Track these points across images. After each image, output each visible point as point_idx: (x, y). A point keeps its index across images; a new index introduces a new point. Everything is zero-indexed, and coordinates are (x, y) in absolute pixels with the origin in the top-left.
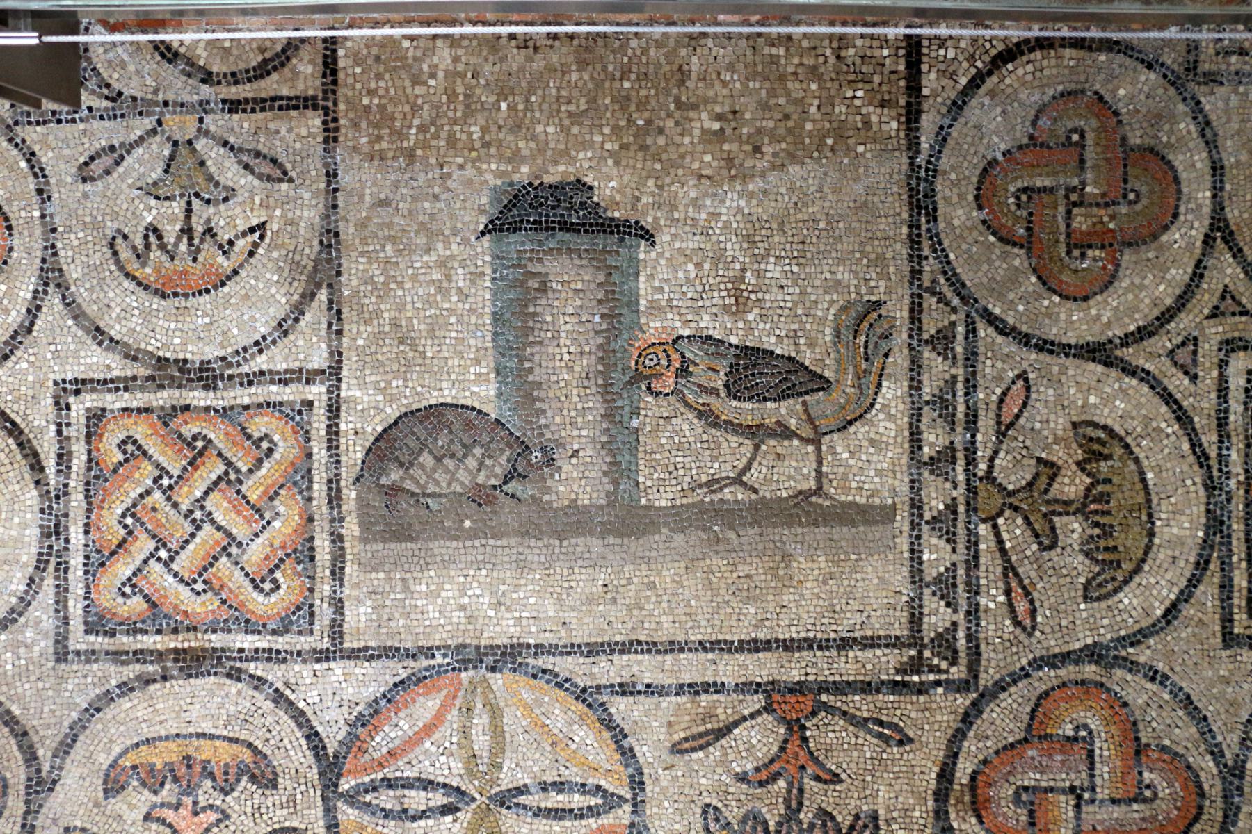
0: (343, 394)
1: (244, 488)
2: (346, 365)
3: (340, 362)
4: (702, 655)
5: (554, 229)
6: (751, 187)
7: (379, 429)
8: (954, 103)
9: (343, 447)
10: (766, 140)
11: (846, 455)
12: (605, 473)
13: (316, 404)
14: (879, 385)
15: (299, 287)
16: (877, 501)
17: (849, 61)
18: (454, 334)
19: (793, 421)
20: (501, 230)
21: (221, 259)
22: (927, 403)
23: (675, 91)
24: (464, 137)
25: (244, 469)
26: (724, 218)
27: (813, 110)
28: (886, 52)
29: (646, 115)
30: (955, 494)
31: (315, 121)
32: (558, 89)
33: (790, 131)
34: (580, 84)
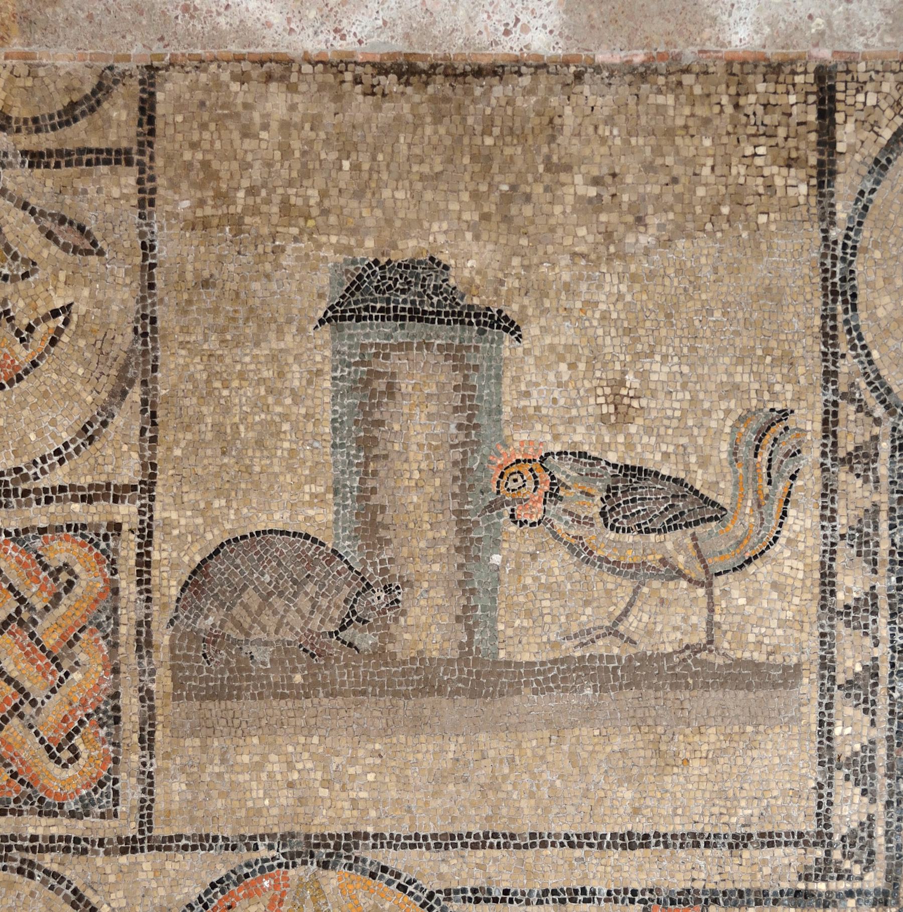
0: (157, 515)
1: (37, 631)
2: (160, 478)
3: (153, 476)
4: (567, 850)
5: (403, 318)
6: (633, 268)
7: (198, 559)
8: (877, 161)
9: (155, 581)
10: (650, 210)
11: (742, 601)
12: (458, 619)
13: (125, 527)
14: (785, 514)
15: (106, 385)
16: (779, 659)
17: (749, 111)
18: (286, 445)
19: (681, 559)
20: (343, 318)
21: (18, 348)
22: (842, 537)
23: (545, 150)
24: (300, 202)
25: (39, 607)
26: (603, 307)
27: (706, 171)
28: (792, 99)
29: (511, 178)
30: (877, 652)
31: (129, 178)
32: (409, 146)
33: (679, 198)
34: (435, 139)
